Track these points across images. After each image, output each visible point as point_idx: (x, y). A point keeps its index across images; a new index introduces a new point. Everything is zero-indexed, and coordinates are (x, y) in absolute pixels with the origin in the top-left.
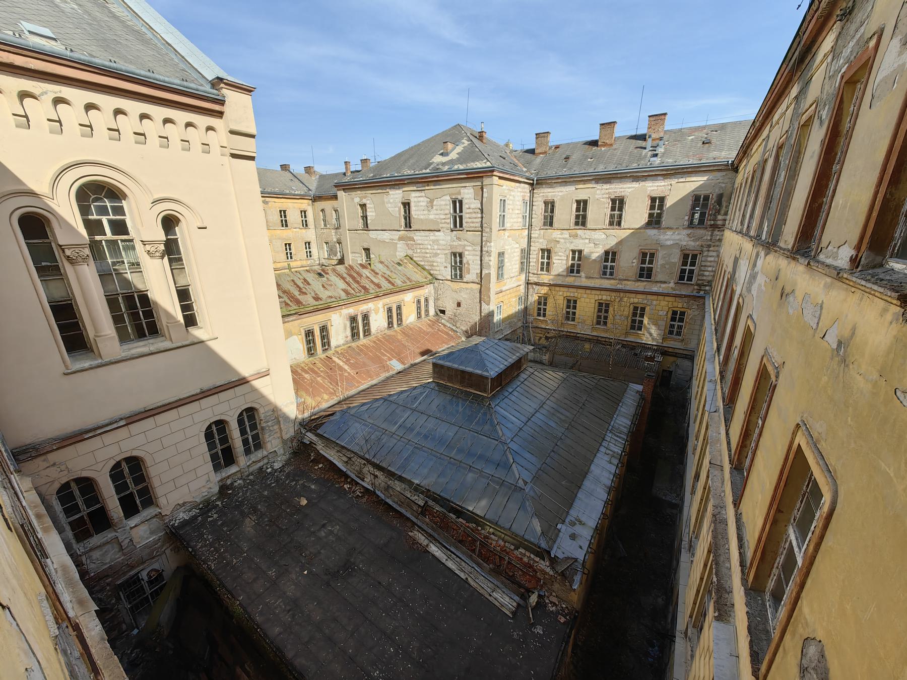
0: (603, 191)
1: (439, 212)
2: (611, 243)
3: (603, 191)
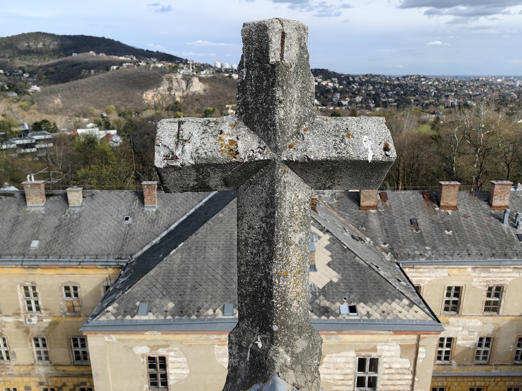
0: (481, 279)
1: (332, 371)
2: (488, 331)
3: (481, 279)
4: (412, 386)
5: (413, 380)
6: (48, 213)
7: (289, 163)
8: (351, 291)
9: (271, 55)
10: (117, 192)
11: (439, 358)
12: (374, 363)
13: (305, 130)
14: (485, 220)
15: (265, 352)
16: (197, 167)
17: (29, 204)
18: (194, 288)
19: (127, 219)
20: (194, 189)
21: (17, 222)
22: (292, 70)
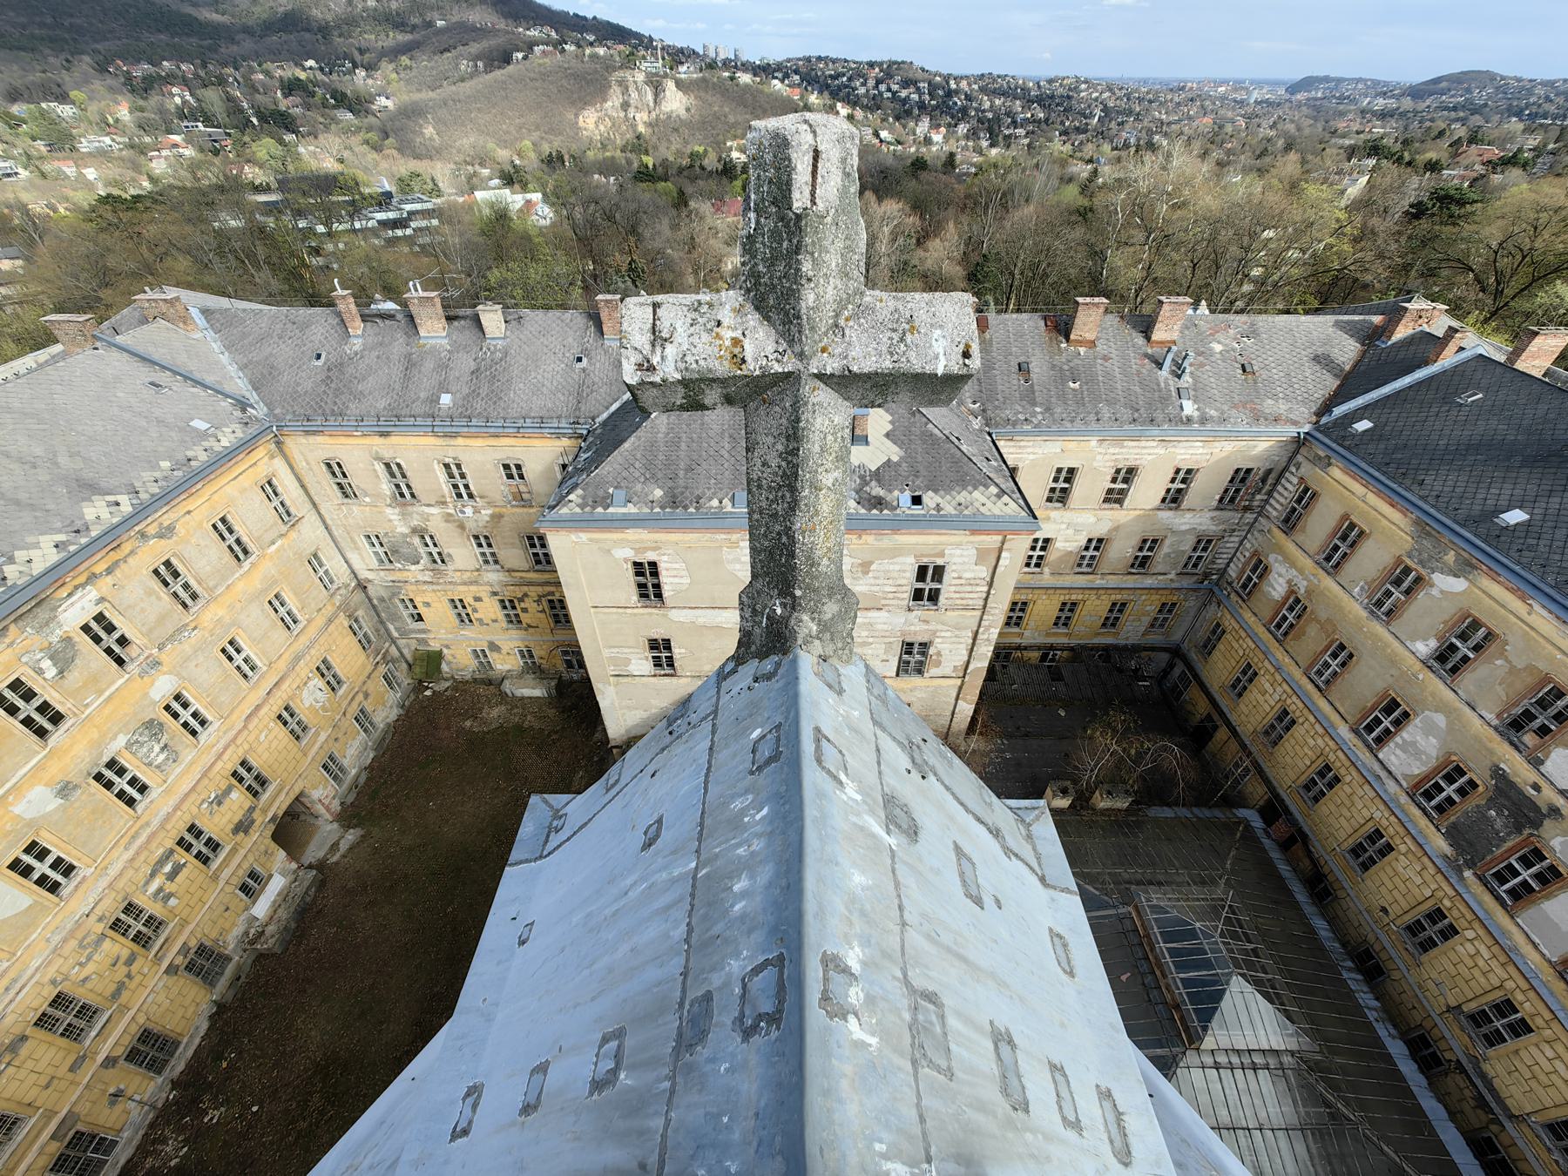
2: (1100, 531)
4: (986, 599)
5: (988, 593)
6: (456, 348)
7: (820, 377)
8: (917, 474)
9: (796, 195)
10: (558, 313)
11: (1028, 565)
12: (939, 572)
13: (847, 320)
14: (1135, 362)
15: (785, 620)
16: (684, 383)
17: (422, 334)
18: (689, 469)
19: (579, 360)
20: (682, 408)
21: (410, 364)
22: (829, 219)
